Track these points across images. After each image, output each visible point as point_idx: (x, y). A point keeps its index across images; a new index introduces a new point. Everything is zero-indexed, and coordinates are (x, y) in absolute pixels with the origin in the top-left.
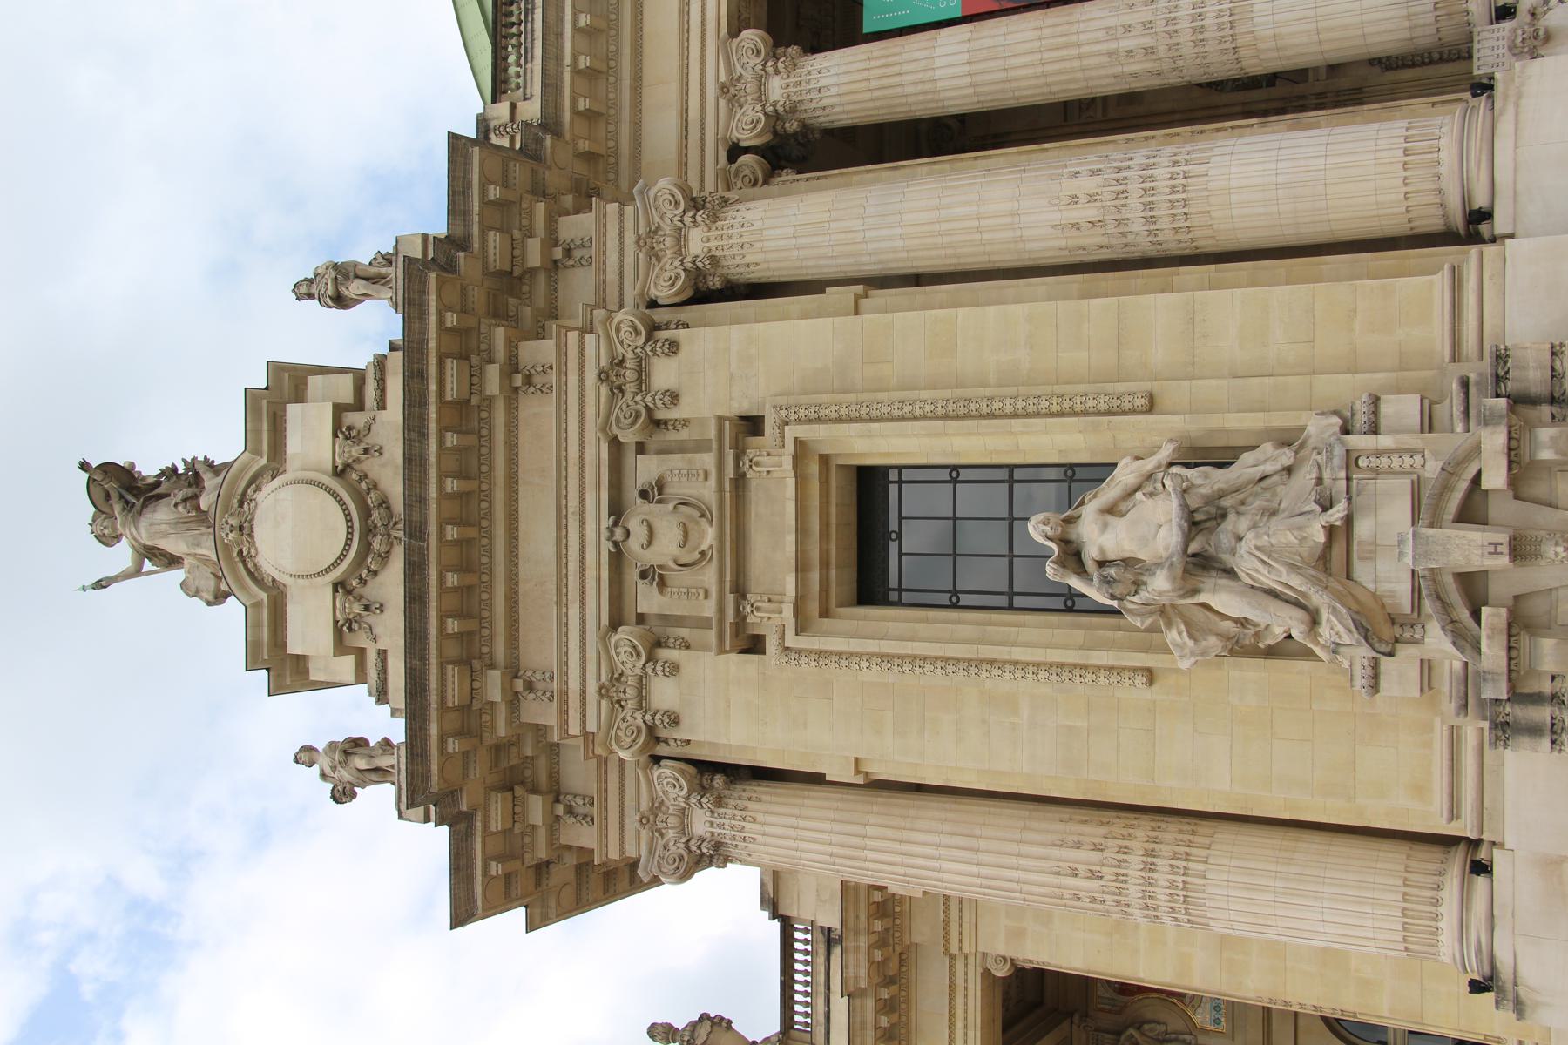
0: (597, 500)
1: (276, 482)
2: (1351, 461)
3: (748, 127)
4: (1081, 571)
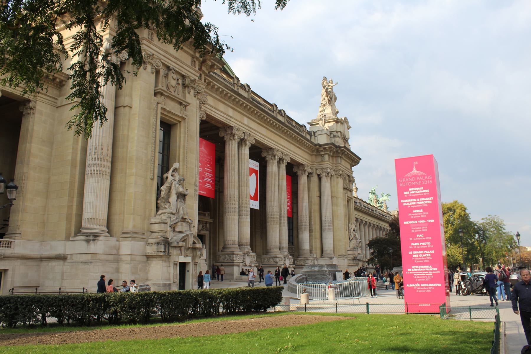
4: (173, 171)
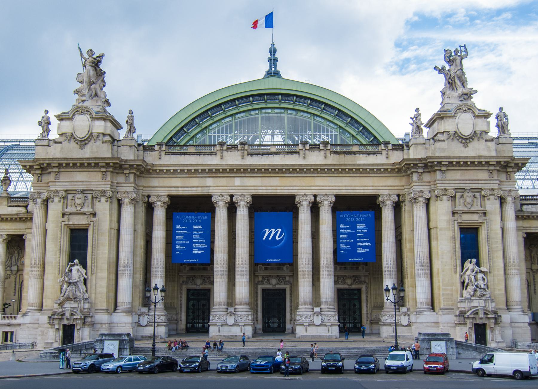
0: (85, 187)
1: (90, 120)
2: (80, 301)
3: (151, 200)
